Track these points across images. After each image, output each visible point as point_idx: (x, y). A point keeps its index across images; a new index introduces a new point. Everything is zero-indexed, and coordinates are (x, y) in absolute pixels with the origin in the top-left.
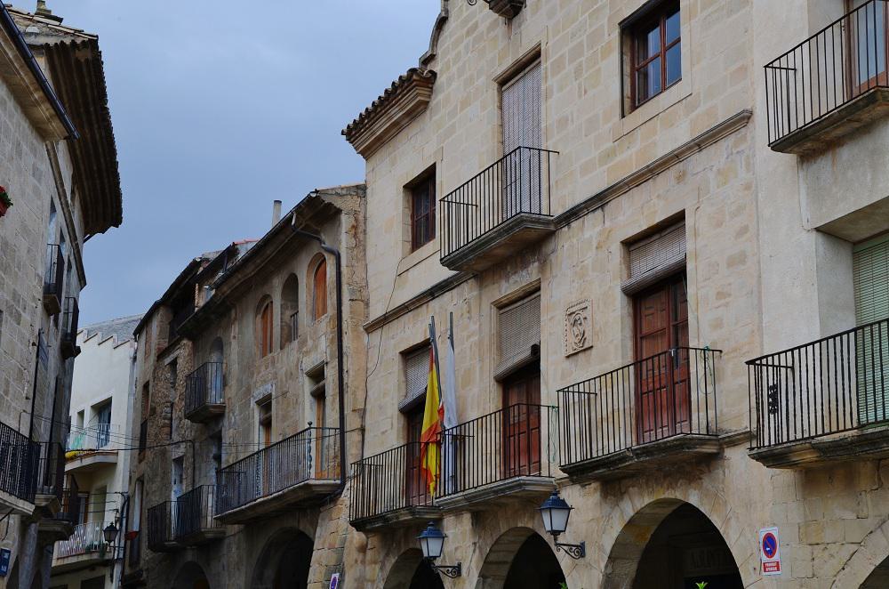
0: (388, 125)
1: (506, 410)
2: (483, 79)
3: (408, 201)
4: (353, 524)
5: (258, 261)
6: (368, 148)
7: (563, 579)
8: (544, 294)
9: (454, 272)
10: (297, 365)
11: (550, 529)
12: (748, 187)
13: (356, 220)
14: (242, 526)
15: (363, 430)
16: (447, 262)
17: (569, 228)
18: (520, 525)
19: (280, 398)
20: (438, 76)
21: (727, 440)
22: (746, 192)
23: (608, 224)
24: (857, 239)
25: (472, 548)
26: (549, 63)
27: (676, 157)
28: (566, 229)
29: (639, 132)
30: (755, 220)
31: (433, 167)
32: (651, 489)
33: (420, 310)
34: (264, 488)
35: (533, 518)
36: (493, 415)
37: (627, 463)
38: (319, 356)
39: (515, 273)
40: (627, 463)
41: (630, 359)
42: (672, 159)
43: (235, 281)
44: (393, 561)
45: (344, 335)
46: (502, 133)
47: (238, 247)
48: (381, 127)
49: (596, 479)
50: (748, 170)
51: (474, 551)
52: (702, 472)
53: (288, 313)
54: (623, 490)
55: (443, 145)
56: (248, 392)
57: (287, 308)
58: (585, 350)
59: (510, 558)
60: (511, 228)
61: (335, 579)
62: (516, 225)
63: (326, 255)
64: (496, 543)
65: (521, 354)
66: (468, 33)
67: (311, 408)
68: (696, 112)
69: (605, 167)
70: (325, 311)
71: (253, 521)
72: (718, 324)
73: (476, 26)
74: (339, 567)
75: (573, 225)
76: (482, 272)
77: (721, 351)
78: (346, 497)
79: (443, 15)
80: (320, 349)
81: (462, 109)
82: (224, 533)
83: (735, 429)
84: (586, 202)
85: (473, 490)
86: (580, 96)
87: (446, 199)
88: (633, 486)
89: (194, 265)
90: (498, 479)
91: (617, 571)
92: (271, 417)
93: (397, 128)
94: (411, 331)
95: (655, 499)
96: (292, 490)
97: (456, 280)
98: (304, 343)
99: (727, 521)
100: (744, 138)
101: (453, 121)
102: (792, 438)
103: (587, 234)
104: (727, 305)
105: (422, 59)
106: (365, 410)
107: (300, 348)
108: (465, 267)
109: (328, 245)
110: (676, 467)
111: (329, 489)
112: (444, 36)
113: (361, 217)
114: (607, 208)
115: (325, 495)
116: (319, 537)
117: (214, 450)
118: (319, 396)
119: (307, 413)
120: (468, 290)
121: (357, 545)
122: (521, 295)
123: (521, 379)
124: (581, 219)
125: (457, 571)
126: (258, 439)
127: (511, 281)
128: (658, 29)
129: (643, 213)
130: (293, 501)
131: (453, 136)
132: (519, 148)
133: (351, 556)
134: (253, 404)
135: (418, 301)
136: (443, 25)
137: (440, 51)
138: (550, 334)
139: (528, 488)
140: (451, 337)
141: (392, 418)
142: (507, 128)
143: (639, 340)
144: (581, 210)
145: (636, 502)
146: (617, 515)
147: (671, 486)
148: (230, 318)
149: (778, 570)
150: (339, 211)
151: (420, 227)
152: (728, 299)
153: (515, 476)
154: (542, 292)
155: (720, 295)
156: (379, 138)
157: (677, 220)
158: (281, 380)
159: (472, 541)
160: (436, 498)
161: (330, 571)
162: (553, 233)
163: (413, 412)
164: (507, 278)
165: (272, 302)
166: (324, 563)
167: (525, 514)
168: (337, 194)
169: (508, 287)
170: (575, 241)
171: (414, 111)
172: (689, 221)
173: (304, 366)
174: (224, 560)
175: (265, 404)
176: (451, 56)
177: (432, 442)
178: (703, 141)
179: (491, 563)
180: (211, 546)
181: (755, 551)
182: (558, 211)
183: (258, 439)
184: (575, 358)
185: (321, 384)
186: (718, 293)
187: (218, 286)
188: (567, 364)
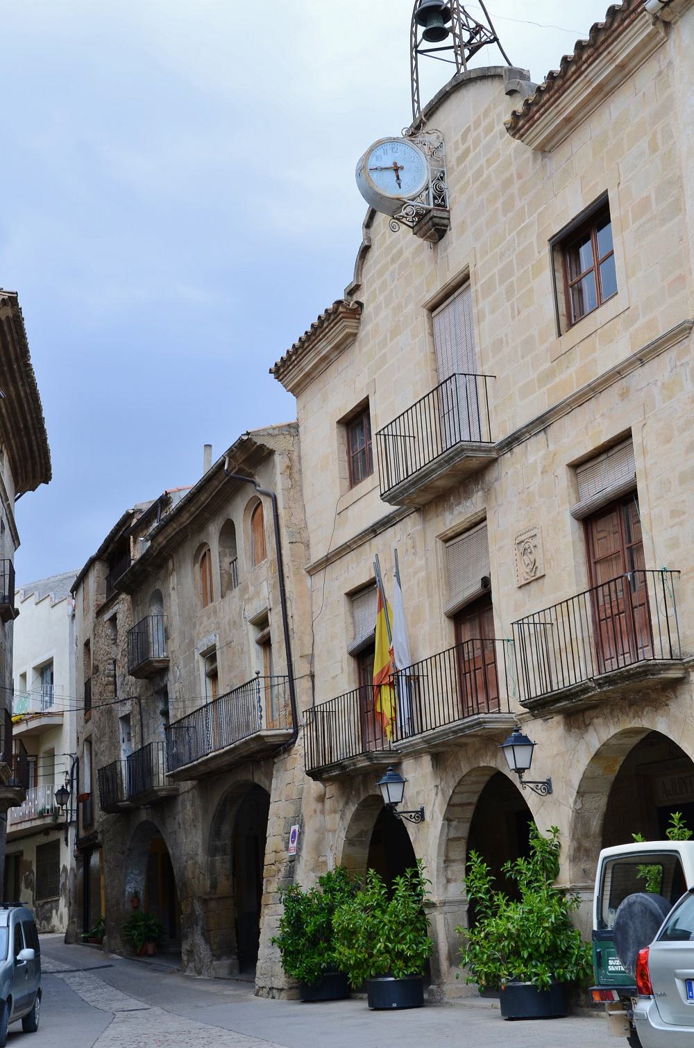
0: (317, 359)
1: (459, 646)
2: (411, 306)
3: (343, 437)
4: (309, 773)
5: (193, 509)
6: (298, 385)
7: (531, 818)
9: (397, 507)
10: (240, 614)
11: (514, 767)
13: (290, 460)
14: (195, 783)
15: (312, 676)
16: (389, 497)
17: (511, 454)
18: (482, 764)
19: (225, 648)
20: (365, 306)
23: (552, 447)
25: (434, 791)
26: (479, 285)
27: (618, 373)
29: (577, 349)
32: (616, 720)
33: (362, 547)
34: (215, 740)
35: (496, 757)
36: (447, 653)
37: (590, 694)
38: (262, 603)
39: (459, 504)
40: (590, 694)
41: (585, 586)
42: (614, 375)
43: (170, 531)
44: (353, 809)
45: (286, 579)
46: (436, 360)
47: (171, 495)
48: (309, 362)
49: (559, 712)
51: (437, 794)
52: (669, 698)
53: (227, 560)
54: (587, 722)
55: (375, 377)
56: (192, 643)
57: (225, 555)
58: (537, 579)
59: (475, 799)
60: (452, 458)
61: (294, 832)
62: (457, 455)
63: (262, 498)
64: (459, 784)
66: (393, 261)
67: (257, 656)
68: (636, 326)
69: (544, 389)
70: (264, 555)
71: (207, 776)
73: (400, 252)
74: (298, 819)
76: (424, 506)
77: (679, 572)
78: (300, 746)
79: (366, 243)
80: (262, 596)
81: (392, 339)
82: (177, 790)
84: (527, 426)
85: (431, 732)
86: (513, 317)
87: (382, 433)
88: (597, 717)
89: (128, 517)
90: (456, 718)
91: (587, 806)
92: (216, 668)
93: (326, 361)
94: (355, 571)
95: (621, 729)
96: (244, 743)
97: (398, 515)
98: (246, 589)
103: (531, 459)
104: (681, 524)
105: (348, 291)
106: (313, 655)
109: (263, 488)
110: (641, 694)
111: (282, 739)
112: (369, 263)
113: (295, 457)
114: (549, 431)
115: (281, 745)
116: (276, 789)
117: (161, 706)
118: (265, 643)
119: (254, 661)
120: (412, 524)
121: (315, 796)
123: (474, 612)
124: (524, 444)
125: (420, 815)
126: (205, 692)
127: (456, 512)
128: (590, 242)
129: (587, 435)
131: (385, 367)
132: (454, 375)
133: (309, 807)
134: (197, 656)
135: (360, 539)
137: (364, 281)
139: (488, 726)
140: (397, 575)
141: (342, 661)
142: (439, 355)
144: (523, 434)
145: (602, 733)
147: (636, 715)
148: (167, 569)
150: (271, 452)
153: (474, 714)
154: (488, 522)
156: (308, 375)
157: (625, 437)
159: (434, 784)
160: (394, 742)
162: (495, 460)
163: (364, 654)
164: (451, 509)
165: (209, 550)
166: (282, 814)
168: (269, 434)
169: (453, 518)
170: (518, 466)
171: (342, 344)
173: (247, 614)
174: (179, 818)
175: (210, 655)
177: (384, 685)
178: (644, 356)
179: (454, 805)
180: (165, 804)
182: (499, 437)
183: (205, 692)
184: (527, 587)
185: (266, 631)
186: (672, 512)
187: (153, 538)
188: (520, 595)
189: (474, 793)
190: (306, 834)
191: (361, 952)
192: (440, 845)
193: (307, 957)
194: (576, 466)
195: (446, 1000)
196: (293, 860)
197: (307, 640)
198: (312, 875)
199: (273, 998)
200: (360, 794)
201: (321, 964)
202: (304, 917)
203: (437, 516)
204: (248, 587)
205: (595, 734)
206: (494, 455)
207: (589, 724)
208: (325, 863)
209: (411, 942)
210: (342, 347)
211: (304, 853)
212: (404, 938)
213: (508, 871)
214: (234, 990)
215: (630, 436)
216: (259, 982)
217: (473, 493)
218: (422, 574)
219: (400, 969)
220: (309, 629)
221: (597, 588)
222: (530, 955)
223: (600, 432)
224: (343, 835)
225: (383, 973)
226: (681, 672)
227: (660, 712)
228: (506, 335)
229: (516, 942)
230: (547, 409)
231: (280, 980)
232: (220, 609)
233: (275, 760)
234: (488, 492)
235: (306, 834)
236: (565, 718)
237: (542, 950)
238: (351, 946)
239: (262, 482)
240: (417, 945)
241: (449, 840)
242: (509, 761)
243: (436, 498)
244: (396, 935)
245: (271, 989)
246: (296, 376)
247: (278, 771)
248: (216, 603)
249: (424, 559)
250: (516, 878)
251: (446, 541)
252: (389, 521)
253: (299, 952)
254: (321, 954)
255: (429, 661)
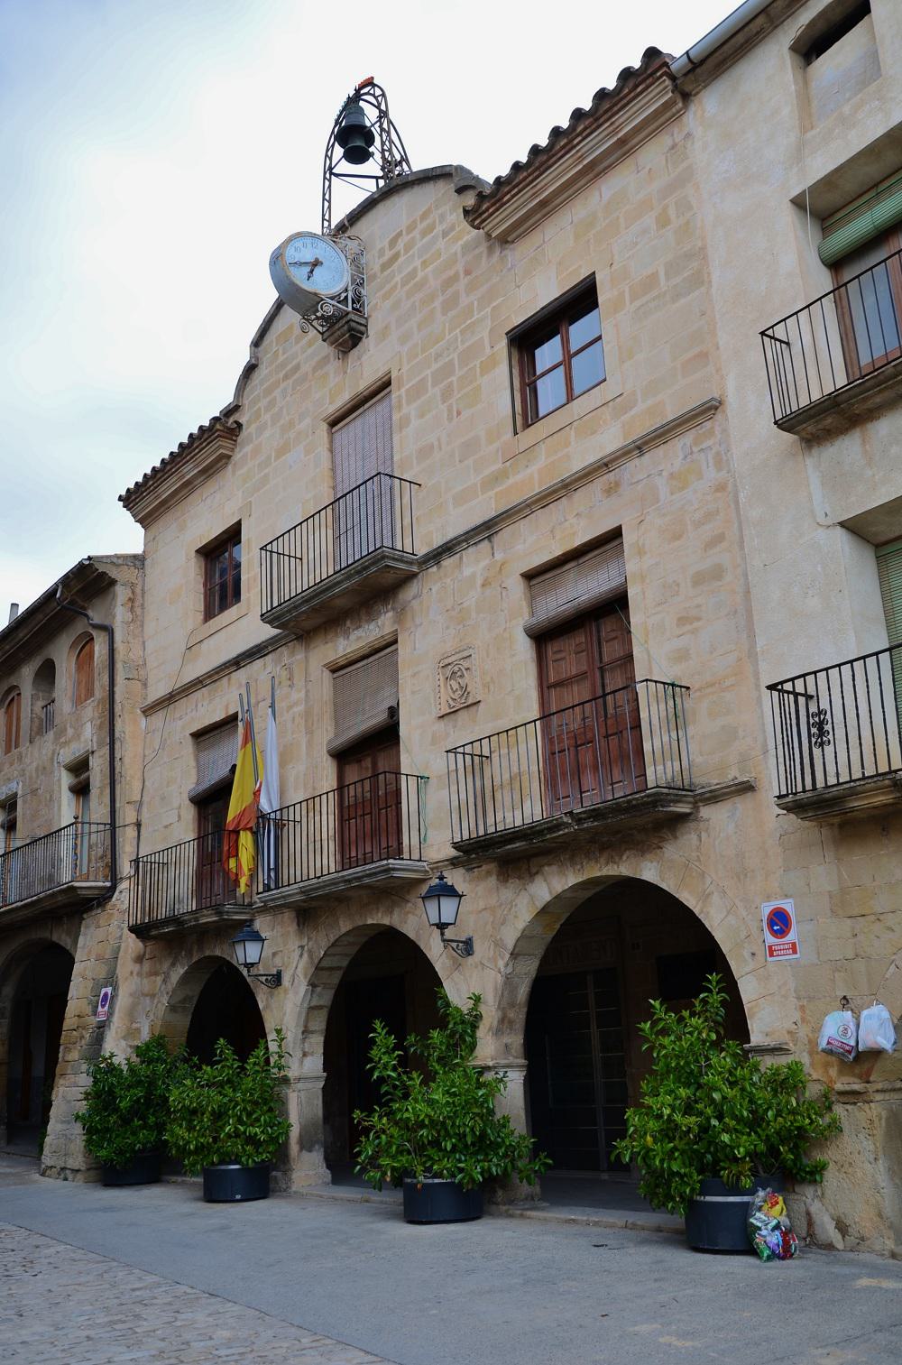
0: (178, 485)
1: (341, 788)
2: (308, 421)
3: (200, 567)
4: (132, 929)
8: (403, 649)
9: (278, 631)
10: (52, 759)
11: (438, 921)
12: (721, 488)
13: (133, 593)
15: (138, 825)
16: (269, 618)
17: (439, 568)
18: (370, 921)
19: (29, 797)
20: (244, 427)
21: (708, 795)
22: (719, 494)
23: (499, 556)
24: (883, 539)
25: (298, 952)
26: (403, 390)
27: (606, 465)
28: (435, 569)
29: (543, 446)
30: (736, 525)
31: (239, 524)
32: (579, 867)
33: (218, 683)
35: (391, 913)
37: (561, 832)
38: (82, 745)
39: (360, 627)
40: (561, 832)
41: (534, 712)
42: (599, 467)
44: (182, 971)
46: (334, 477)
48: (166, 489)
49: (495, 860)
50: (719, 469)
51: (301, 956)
52: (663, 840)
53: (40, 703)
54: (534, 870)
55: (252, 499)
57: (38, 699)
58: (468, 706)
59: (345, 963)
61: (106, 995)
62: (373, 564)
63: (94, 633)
64: (333, 945)
65: (371, 718)
66: (286, 377)
67: (69, 805)
68: (633, 412)
69: (491, 493)
72: (681, 656)
73: (297, 367)
74: (111, 980)
75: (444, 563)
76: (308, 632)
77: (688, 688)
78: (124, 897)
79: (253, 361)
80: (86, 736)
81: (277, 457)
83: (716, 781)
85: (315, 881)
86: (450, 419)
87: (269, 548)
88: (550, 865)
90: (332, 870)
91: (517, 970)
92: (15, 819)
93: (189, 487)
94: (208, 709)
95: (585, 878)
97: (271, 644)
99: (705, 897)
100: (711, 433)
101: (266, 471)
102: (857, 775)
103: (467, 571)
104: (694, 632)
105: (224, 412)
106: (141, 803)
107: (57, 738)
108: (292, 624)
111: (96, 892)
112: (253, 384)
113: (138, 590)
114: (496, 539)
115: (93, 899)
116: (83, 948)
118: (81, 790)
119: (66, 809)
120: (293, 657)
121: (133, 956)
122: (365, 652)
123: (370, 751)
124: (458, 555)
125: (276, 980)
127: (353, 637)
128: (558, 338)
129: (554, 538)
130: (48, 908)
131: (265, 488)
133: (126, 967)
135: (217, 673)
136: (251, 373)
137: (246, 402)
138: (413, 693)
139: (397, 874)
140: (272, 706)
142: (339, 472)
143: (545, 689)
144: (459, 543)
146: (525, 901)
147: (611, 860)
149: (795, 952)
150: (113, 582)
151: (215, 596)
152: (696, 624)
153: (381, 860)
154: (400, 645)
155: (682, 621)
157: (616, 534)
158: (31, 778)
159: (298, 943)
160: (258, 894)
161: (98, 985)
162: (415, 575)
163: (212, 801)
164: (347, 635)
165: (19, 694)
166: (89, 974)
167: (378, 909)
168: (112, 563)
169: (345, 645)
171: (212, 467)
172: (628, 538)
173: (61, 758)
176: (263, 403)
178: (646, 443)
179: (322, 969)
181: (755, 932)
182: (422, 550)
184: (452, 715)
185: (83, 776)
186: (680, 619)
188: (441, 725)
189: (346, 955)
190: (120, 998)
191: (203, 1135)
192: (300, 1013)
193: (117, 1136)
194: (530, 576)
195: (294, 1189)
196: (102, 1027)
197: (137, 785)
198: (123, 1043)
199: (66, 1179)
200: (192, 955)
201: (135, 1145)
202: (117, 1090)
203: (326, 643)
204: (66, 730)
205: (544, 885)
206: (415, 569)
207: (537, 873)
208: (138, 1030)
209: (267, 1124)
210: (211, 472)
211: (115, 1018)
212: (258, 1120)
213: (412, 1046)
214: (8, 1166)
215: (621, 535)
216: (48, 1159)
217: (379, 614)
218: (300, 708)
219: (249, 1156)
220: (139, 774)
221: (604, 695)
222: (454, 1146)
223: (574, 534)
224: (165, 1000)
225: (227, 1159)
226: (690, 806)
227: (648, 856)
228: (439, 440)
229: (438, 1132)
230: (494, 514)
231: (77, 1160)
232: (27, 754)
233: (85, 916)
234: (400, 616)
235: (119, 1001)
236: (500, 866)
237: (469, 1140)
238: (191, 1128)
239: (96, 615)
240: (271, 1128)
241: (311, 1009)
242: (415, 922)
243: (325, 623)
244: (249, 1115)
245: (63, 1169)
246: (150, 503)
247: (86, 927)
248: (22, 749)
249: (303, 692)
250: (422, 1053)
251: (333, 671)
252: (259, 651)
253: (108, 1130)
254: (134, 1133)
255: (304, 804)
